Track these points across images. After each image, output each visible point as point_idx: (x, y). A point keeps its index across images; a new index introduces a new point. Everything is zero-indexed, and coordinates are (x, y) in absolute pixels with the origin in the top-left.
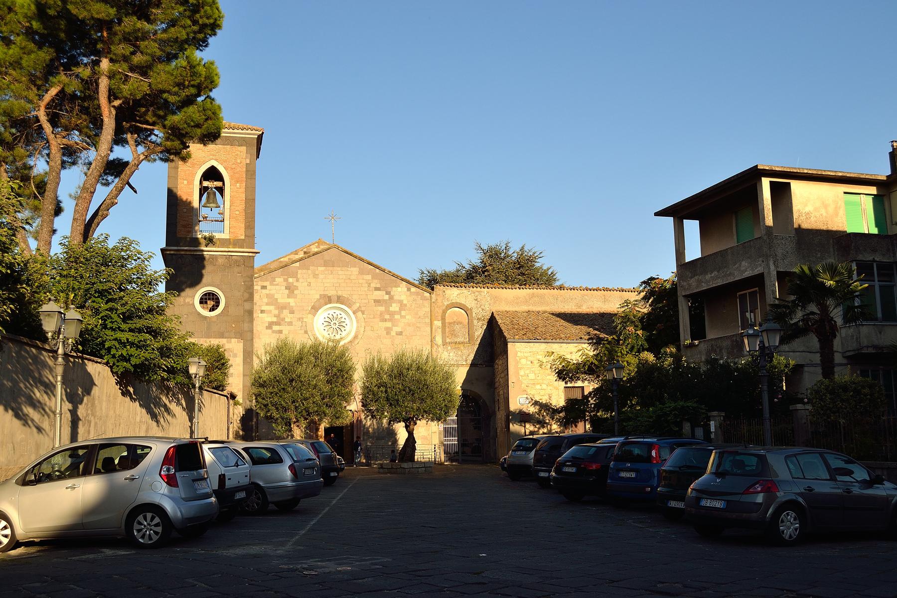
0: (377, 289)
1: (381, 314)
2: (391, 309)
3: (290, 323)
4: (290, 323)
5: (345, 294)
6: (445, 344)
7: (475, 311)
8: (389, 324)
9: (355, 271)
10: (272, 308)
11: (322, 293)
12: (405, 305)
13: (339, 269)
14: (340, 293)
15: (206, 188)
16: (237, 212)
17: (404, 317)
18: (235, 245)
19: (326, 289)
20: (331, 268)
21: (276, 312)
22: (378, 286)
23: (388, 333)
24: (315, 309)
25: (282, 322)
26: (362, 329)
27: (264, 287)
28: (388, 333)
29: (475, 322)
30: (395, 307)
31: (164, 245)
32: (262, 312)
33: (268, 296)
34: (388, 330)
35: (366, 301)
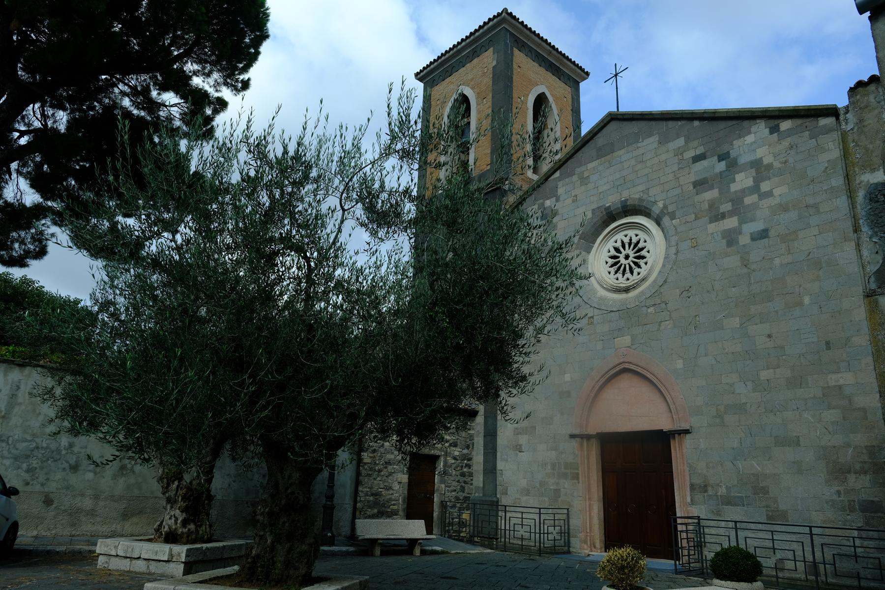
0: (697, 159)
1: (712, 205)
2: (734, 187)
5: (633, 194)
8: (731, 223)
9: (649, 144)
11: (595, 206)
12: (770, 166)
13: (621, 152)
19: (601, 196)
22: (699, 152)
30: (743, 180)
34: (731, 238)
35: (678, 191)
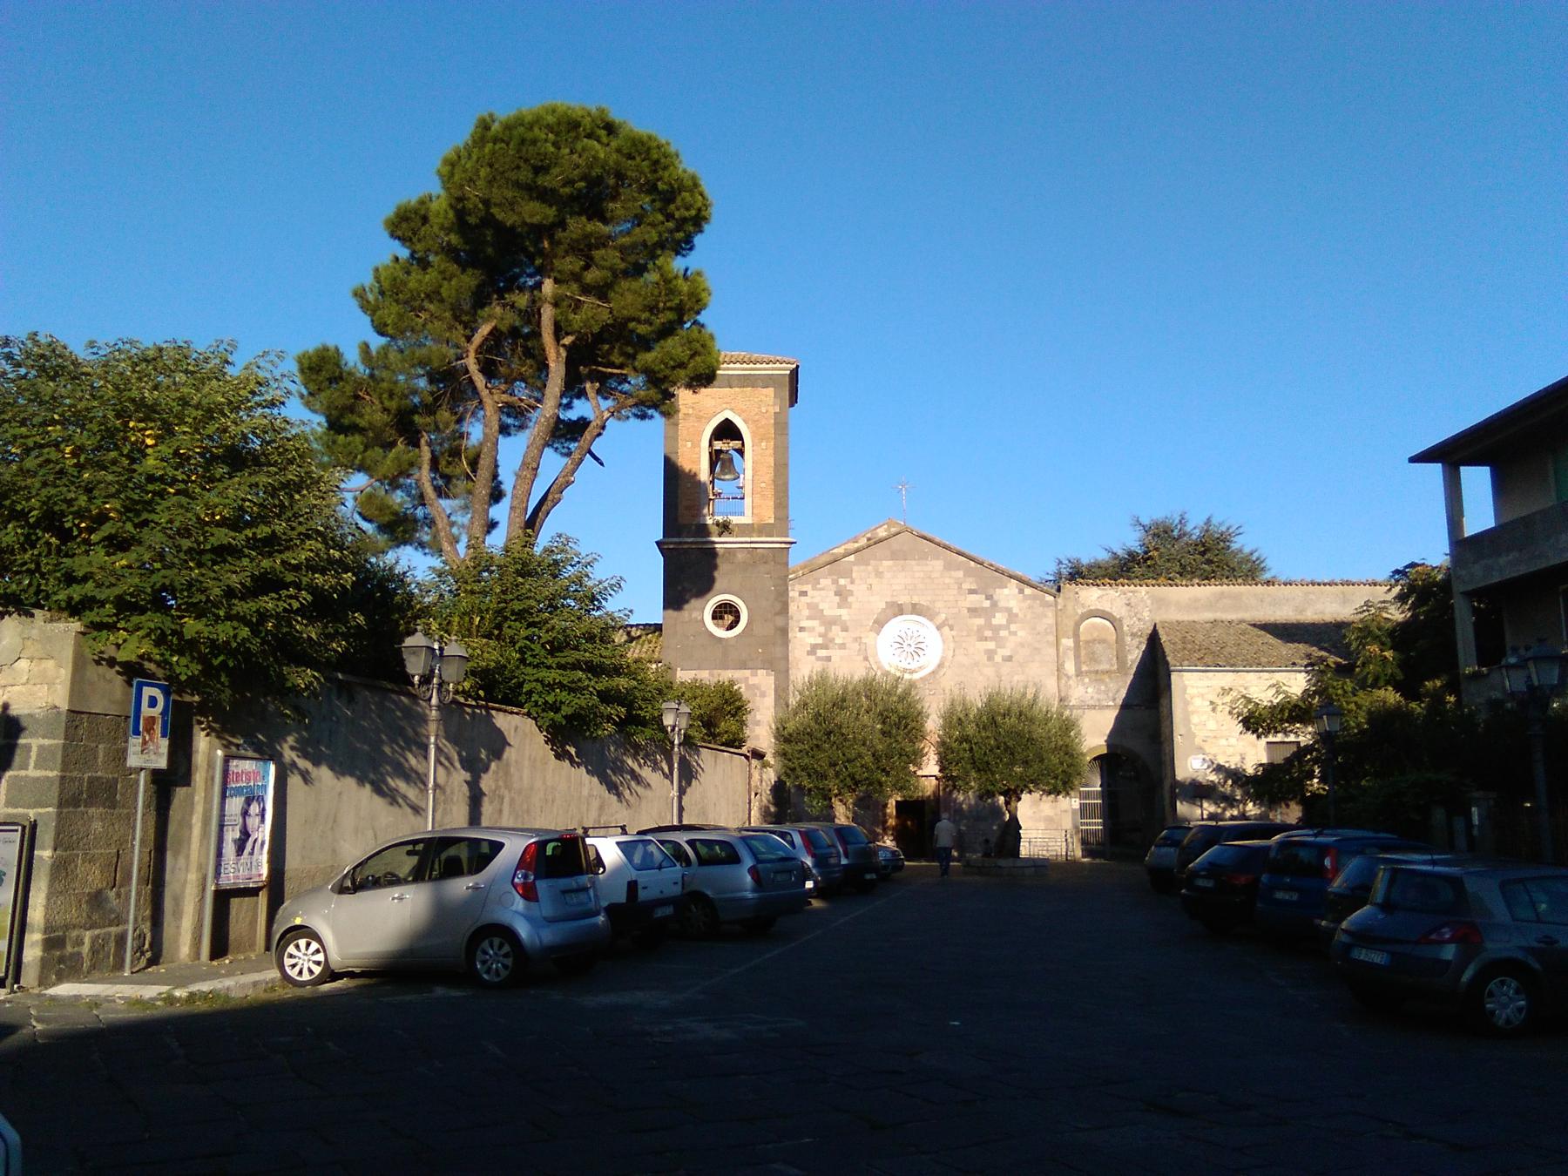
0: (972, 592)
1: (980, 629)
2: (995, 621)
3: (842, 646)
4: (842, 646)
6: (1079, 673)
7: (1126, 622)
8: (991, 645)
9: (938, 565)
10: (815, 623)
12: (1016, 615)
13: (913, 562)
14: (916, 600)
15: (719, 452)
16: (763, 485)
17: (1015, 633)
18: (760, 534)
20: (902, 562)
21: (822, 629)
22: (974, 587)
23: (990, 658)
24: (879, 624)
25: (831, 645)
26: (951, 653)
27: (804, 593)
28: (990, 658)
29: (1128, 639)
30: (1000, 619)
31: (660, 537)
32: (802, 629)
33: (809, 606)
34: (990, 655)
35: (956, 610)
